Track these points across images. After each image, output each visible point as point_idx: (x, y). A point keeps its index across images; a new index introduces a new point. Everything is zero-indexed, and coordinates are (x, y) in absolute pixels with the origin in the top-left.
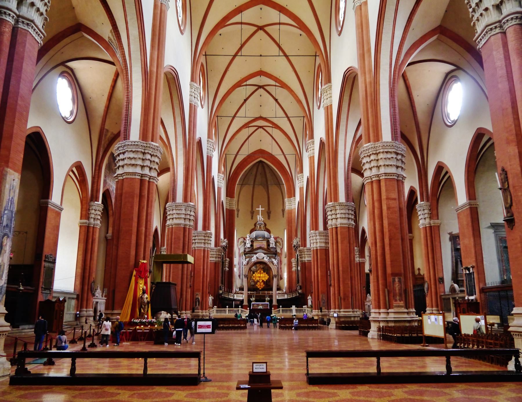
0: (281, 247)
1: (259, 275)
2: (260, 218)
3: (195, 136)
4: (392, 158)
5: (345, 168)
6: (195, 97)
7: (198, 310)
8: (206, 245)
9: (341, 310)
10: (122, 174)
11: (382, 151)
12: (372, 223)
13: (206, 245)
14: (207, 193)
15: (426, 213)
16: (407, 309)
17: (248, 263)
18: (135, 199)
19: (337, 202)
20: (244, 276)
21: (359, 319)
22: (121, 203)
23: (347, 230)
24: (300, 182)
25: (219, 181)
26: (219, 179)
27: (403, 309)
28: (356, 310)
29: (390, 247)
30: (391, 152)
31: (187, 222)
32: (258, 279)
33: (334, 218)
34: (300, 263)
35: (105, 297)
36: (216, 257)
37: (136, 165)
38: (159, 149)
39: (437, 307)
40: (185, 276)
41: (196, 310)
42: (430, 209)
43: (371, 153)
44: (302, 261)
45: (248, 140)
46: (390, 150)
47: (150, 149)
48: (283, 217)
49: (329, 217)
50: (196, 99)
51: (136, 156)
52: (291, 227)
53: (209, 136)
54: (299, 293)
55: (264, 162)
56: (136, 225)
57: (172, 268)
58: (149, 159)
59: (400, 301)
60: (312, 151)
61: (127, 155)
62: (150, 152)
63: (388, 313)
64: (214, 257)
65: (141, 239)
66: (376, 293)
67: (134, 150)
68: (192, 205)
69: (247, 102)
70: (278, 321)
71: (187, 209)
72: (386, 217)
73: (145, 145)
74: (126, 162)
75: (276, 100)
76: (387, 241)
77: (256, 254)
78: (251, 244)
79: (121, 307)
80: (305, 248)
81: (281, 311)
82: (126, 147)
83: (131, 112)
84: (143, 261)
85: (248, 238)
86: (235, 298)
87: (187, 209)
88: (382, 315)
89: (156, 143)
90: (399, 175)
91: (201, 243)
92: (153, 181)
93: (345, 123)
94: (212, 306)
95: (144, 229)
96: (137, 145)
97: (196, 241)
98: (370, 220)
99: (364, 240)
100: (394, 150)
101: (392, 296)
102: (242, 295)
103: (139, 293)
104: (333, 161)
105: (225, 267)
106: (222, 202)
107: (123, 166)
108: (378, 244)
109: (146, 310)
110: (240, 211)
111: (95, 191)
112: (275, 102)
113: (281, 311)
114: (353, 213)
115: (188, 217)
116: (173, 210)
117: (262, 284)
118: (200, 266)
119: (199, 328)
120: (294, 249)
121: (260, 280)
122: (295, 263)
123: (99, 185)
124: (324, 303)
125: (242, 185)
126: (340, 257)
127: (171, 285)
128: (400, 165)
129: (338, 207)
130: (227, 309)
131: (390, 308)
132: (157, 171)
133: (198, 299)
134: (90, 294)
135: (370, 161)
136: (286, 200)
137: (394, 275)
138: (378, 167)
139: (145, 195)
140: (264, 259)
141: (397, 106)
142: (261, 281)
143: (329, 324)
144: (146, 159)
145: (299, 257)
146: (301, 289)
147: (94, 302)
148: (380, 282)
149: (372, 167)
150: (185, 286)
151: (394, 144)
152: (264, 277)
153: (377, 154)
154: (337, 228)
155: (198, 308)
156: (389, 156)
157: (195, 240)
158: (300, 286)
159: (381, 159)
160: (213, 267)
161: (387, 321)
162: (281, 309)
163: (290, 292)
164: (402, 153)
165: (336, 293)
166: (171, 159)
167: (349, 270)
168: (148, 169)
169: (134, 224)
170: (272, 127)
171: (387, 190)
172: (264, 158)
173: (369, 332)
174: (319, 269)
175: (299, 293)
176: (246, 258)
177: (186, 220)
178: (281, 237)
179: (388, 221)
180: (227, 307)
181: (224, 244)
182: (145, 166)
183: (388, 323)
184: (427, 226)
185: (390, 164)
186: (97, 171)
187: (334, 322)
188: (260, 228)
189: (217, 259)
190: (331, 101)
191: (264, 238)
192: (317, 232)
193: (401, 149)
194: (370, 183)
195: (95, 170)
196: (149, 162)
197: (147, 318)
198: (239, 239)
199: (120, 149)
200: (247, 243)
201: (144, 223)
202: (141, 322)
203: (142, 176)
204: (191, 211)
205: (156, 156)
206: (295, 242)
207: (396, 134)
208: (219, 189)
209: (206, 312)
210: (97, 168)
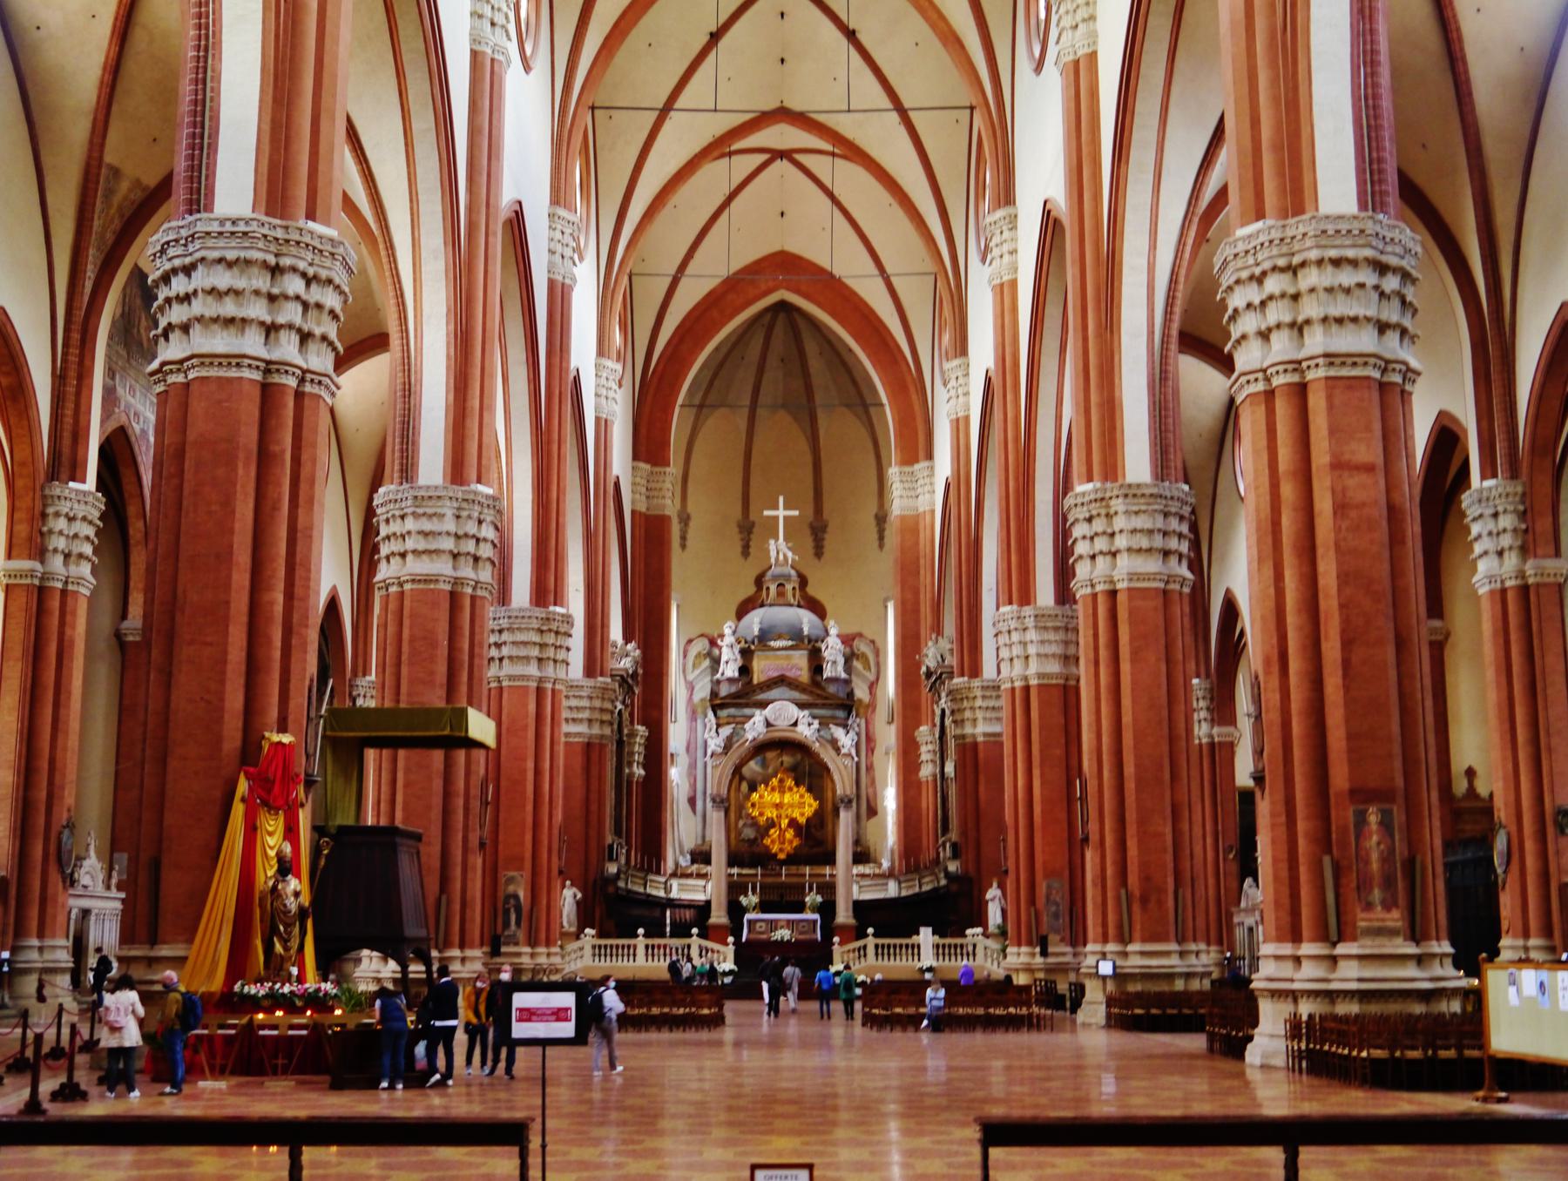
0: (872, 677)
1: (776, 798)
2: (779, 551)
3: (499, 194)
4: (1361, 286)
5: (1151, 333)
6: (493, 24)
7: (516, 944)
8: (550, 671)
9: (1130, 948)
10: (181, 362)
11: (1313, 255)
12: (1269, 572)
13: (550, 671)
14: (549, 442)
15: (1505, 530)
16: (1418, 943)
17: (727, 747)
18: (241, 472)
19: (1115, 480)
20: (714, 800)
21: (1207, 984)
22: (180, 487)
23: (1160, 600)
24: (953, 393)
25: (604, 392)
26: (603, 381)
27: (1399, 940)
28: (1193, 947)
29: (1345, 675)
30: (1354, 263)
31: (466, 571)
32: (771, 813)
33: (1101, 553)
34: (951, 745)
35: (119, 888)
36: (590, 721)
37: (244, 320)
38: (341, 250)
39: (1547, 932)
40: (460, 802)
41: (507, 944)
42: (1525, 512)
43: (1267, 265)
44: (963, 737)
45: (726, 212)
46: (1350, 253)
47: (303, 253)
48: (881, 546)
49: (1082, 548)
50: (498, 30)
51: (240, 284)
52: (916, 592)
53: (558, 196)
54: (947, 875)
55: (798, 310)
56: (247, 583)
57: (401, 764)
58: (298, 298)
59: (1387, 907)
60: (1006, 258)
61: (201, 279)
62: (302, 265)
63: (1333, 960)
64: (581, 720)
65: (269, 642)
66: (1284, 874)
67: (231, 255)
68: (487, 497)
69: (724, 43)
70: (858, 991)
71: (464, 514)
72: (1332, 543)
73: (280, 234)
74: (198, 307)
75: (851, 35)
76: (1332, 649)
77: (763, 705)
78: (740, 663)
79: (189, 933)
80: (976, 683)
81: (871, 951)
82: (197, 244)
83: (217, 91)
84: (276, 738)
86: (674, 894)
87: (464, 514)
88: (1309, 970)
89: (327, 223)
90: (1387, 362)
91: (527, 659)
92: (315, 390)
93: (1152, 136)
94: (573, 929)
95: (279, 598)
96: (245, 234)
97: (505, 651)
98: (1260, 560)
99: (1232, 647)
100: (1368, 253)
101: (1354, 884)
102: (702, 882)
103: (266, 873)
104: (1098, 301)
105: (630, 764)
106: (617, 485)
107: (185, 328)
108: (1295, 665)
109: (294, 944)
110: (692, 524)
111: (67, 436)
112: (844, 41)
113: (871, 951)
114: (1185, 529)
115: (470, 546)
116: (402, 517)
117: (790, 834)
118: (524, 760)
119: (520, 1020)
120: (925, 685)
121: (779, 817)
122: (930, 747)
123: (83, 408)
124: (1056, 916)
125: (701, 408)
126: (1127, 718)
127: (398, 840)
128: (1394, 317)
129: (1118, 505)
130: (641, 942)
131: (1341, 938)
132: (335, 349)
133: (516, 897)
134: (55, 877)
135: (1263, 304)
136: (893, 471)
137: (1361, 795)
138: (1298, 328)
139: (283, 451)
141: (1384, 57)
142: (785, 823)
143: (1076, 1005)
144: (286, 297)
145: (948, 722)
146: (955, 855)
147: (74, 912)
148: (1302, 826)
149: (1270, 330)
150: (460, 844)
151: (1370, 227)
152: (800, 804)
153: (1293, 270)
154: (1113, 594)
155: (514, 935)
156: (1347, 277)
157: (498, 645)
158: (954, 846)
159: (1312, 290)
160: (578, 762)
161: (1331, 996)
162: (871, 941)
163: (908, 871)
164: (1404, 263)
165: (1110, 871)
166: (392, 294)
167: (1167, 776)
168: (295, 338)
169: (235, 576)
170: (833, 154)
171: (1333, 431)
172: (798, 291)
173: (1250, 1038)
174: (1036, 772)
175: (947, 875)
176: (718, 726)
177: (462, 559)
178: (868, 633)
179: (1339, 564)
180: (641, 931)
181: (626, 664)
182: (282, 326)
183: (1333, 1002)
184: (1509, 584)
185: (1352, 313)
186: (74, 351)
187: (1101, 997)
188: (781, 594)
189: (596, 730)
190: (1093, 36)
191: (797, 637)
192: (1028, 611)
193: (1398, 250)
194: (1262, 398)
195: (66, 345)
196: (300, 309)
197: (301, 979)
198: (690, 641)
199: (171, 252)
200: (724, 658)
201: (281, 573)
202: (272, 995)
203: (267, 372)
204: (480, 522)
205: (330, 281)
206: (931, 656)
207: (1380, 181)
208: (603, 425)
209: (549, 955)
210: (76, 336)
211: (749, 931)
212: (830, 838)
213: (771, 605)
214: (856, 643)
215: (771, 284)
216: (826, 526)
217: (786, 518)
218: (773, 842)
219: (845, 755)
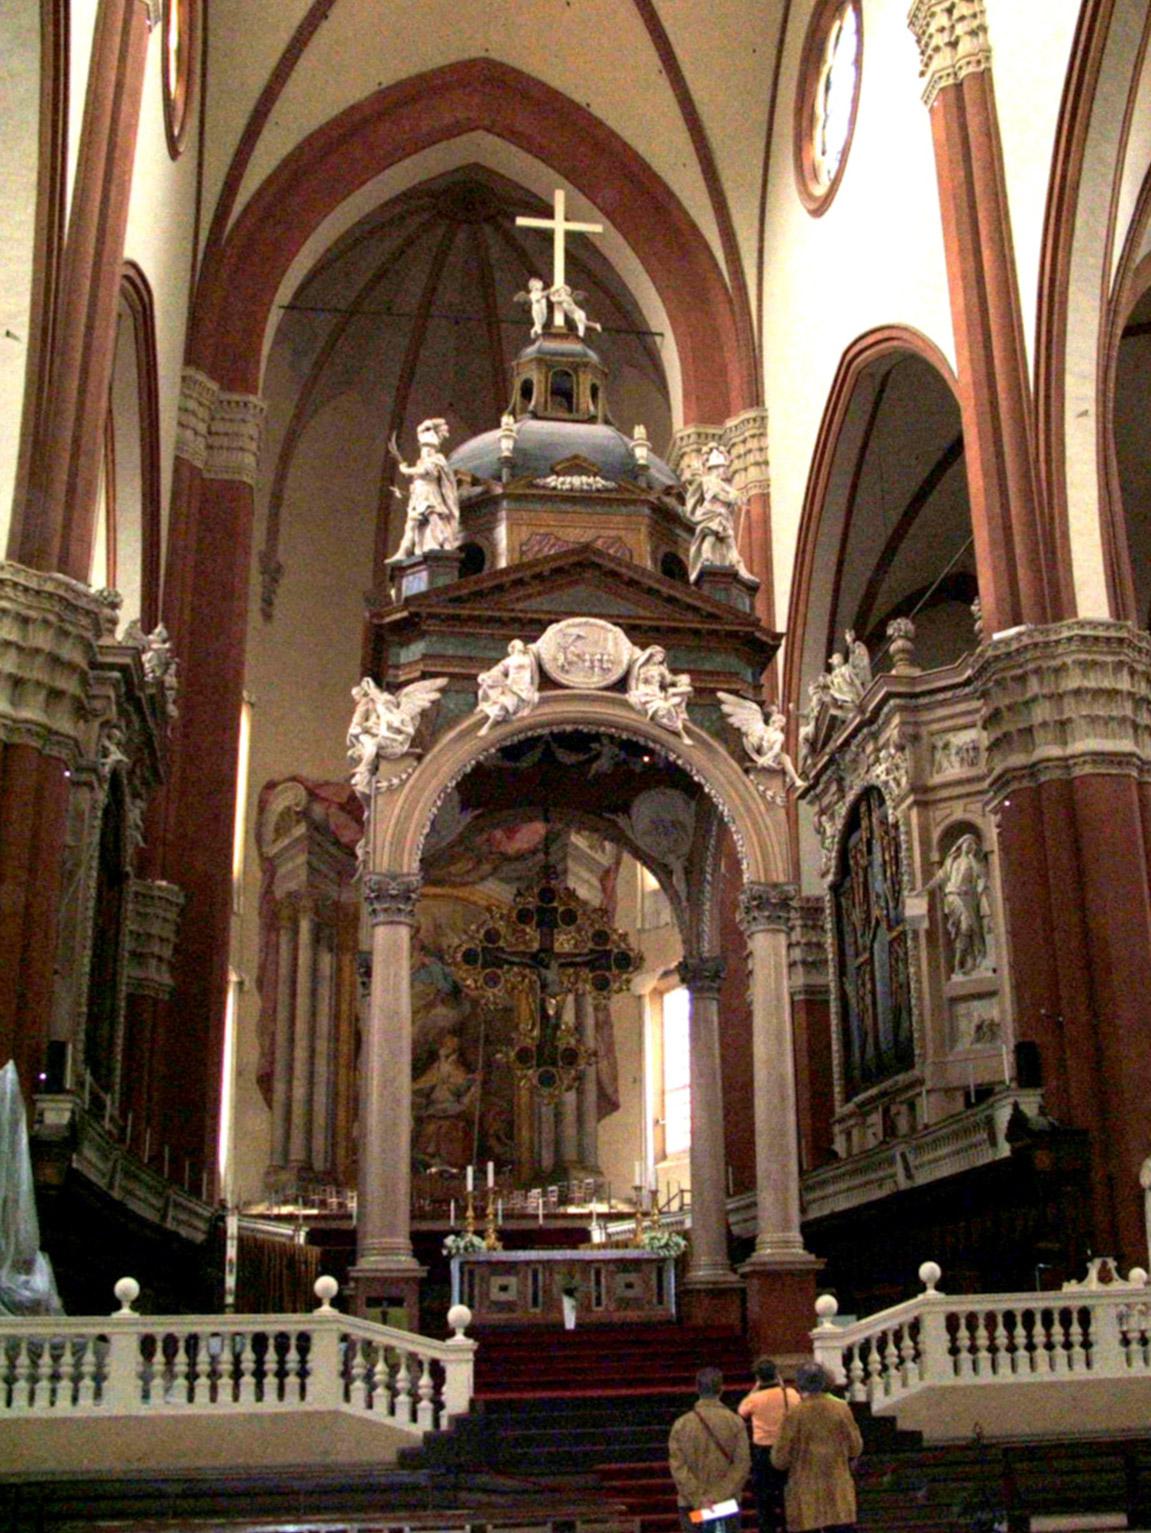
17: (422, 741)
44: (1032, 770)
77: (531, 630)
81: (934, 1337)
85: (429, 460)
110: (284, 581)
113: (934, 1337)
140: (636, 694)
162: (931, 1305)
198: (271, 786)
212: (525, 1155)
213: (535, 416)
217: (569, 235)
219: (767, 771)
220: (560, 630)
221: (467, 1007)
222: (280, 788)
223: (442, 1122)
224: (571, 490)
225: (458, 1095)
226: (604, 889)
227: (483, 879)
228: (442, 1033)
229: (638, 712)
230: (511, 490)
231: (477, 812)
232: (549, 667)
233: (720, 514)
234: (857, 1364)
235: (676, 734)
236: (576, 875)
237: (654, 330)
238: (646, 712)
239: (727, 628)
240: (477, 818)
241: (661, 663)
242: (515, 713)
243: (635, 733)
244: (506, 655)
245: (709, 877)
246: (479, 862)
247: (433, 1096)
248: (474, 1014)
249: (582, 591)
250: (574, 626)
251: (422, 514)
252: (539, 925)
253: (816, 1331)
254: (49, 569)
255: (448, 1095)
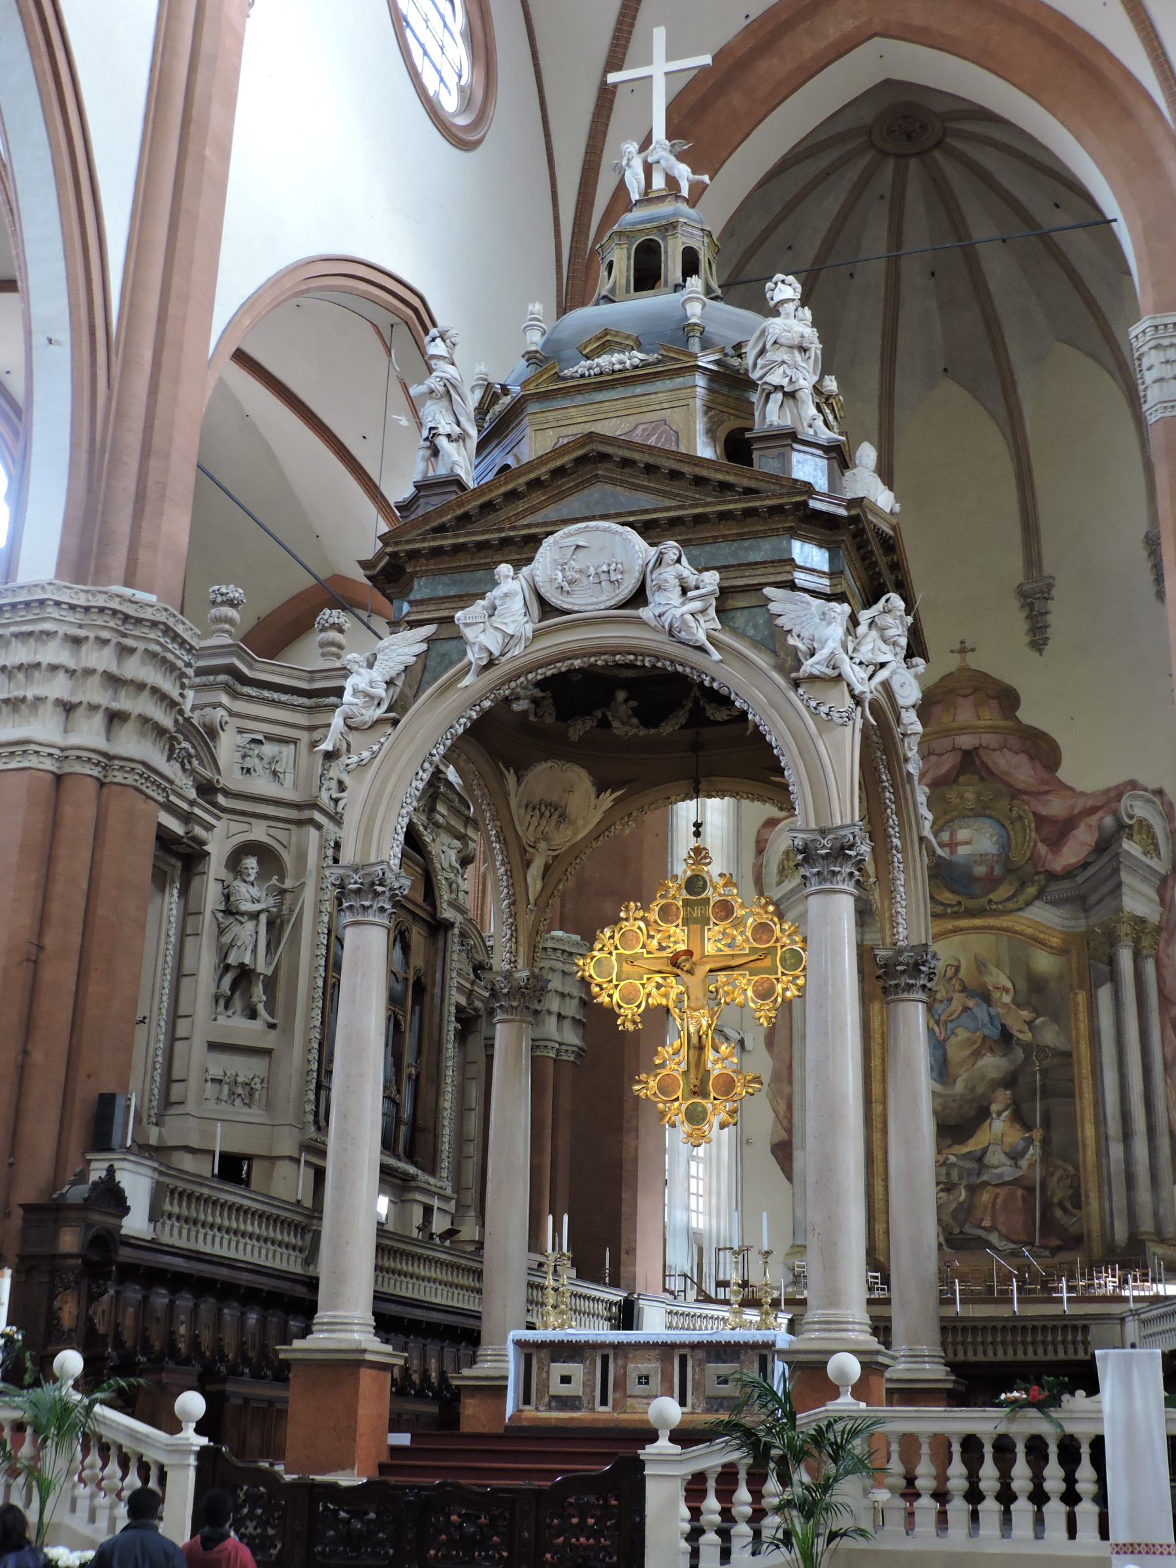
36: (68, 708)
211: (527, 1401)
212: (1095, 1227)
214: (1125, 802)
215: (849, 25)
216: (1050, 586)
218: (663, 1089)
219: (812, 678)
220: (556, 542)
221: (1020, 1054)
222: (779, 826)
223: (997, 1190)
224: (601, 373)
225: (1015, 1156)
226: (1162, 902)
227: (1028, 904)
228: (995, 1084)
229: (654, 629)
230: (532, 389)
231: (618, 793)
232: (542, 591)
233: (783, 362)
234: (712, 1503)
235: (701, 649)
236: (1133, 889)
237: (1110, 217)
238: (663, 627)
239: (768, 503)
240: (617, 801)
241: (679, 561)
242: (502, 655)
243: (658, 658)
244: (495, 584)
245: (896, 841)
246: (1023, 885)
247: (986, 1160)
248: (1027, 1059)
249: (596, 492)
250: (570, 535)
251: (426, 439)
252: (686, 922)
253: (650, 1449)
254: (109, 583)
255: (1004, 1158)
